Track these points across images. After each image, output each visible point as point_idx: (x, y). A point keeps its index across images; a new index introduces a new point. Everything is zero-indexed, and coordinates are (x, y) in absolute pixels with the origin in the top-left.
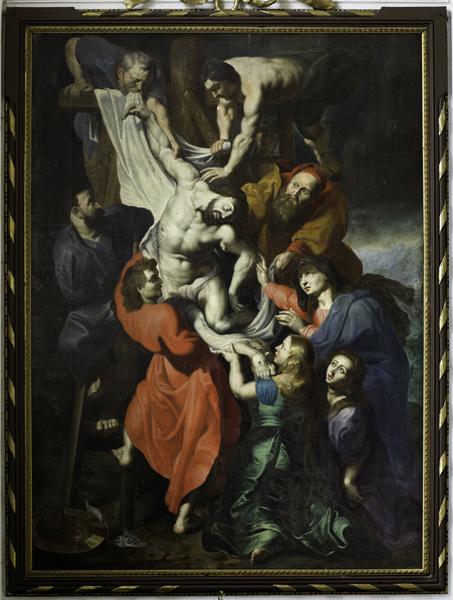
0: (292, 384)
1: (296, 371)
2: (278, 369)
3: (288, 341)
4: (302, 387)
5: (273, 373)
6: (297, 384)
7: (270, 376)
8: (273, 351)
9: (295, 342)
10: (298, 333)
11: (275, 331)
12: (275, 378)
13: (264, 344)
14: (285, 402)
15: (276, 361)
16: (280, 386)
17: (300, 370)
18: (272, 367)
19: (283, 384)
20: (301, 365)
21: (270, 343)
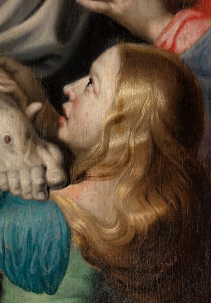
0: (120, 215)
1: (138, 171)
2: (73, 164)
3: (108, 64)
4: (159, 227)
5: (54, 175)
6: (142, 217)
7: (46, 187)
8: (57, 99)
9: (132, 66)
10: (141, 38)
11: (63, 29)
12: (61, 196)
13: (24, 73)
14: (97, 280)
15: (64, 133)
16: (78, 224)
17: (150, 170)
18: (51, 157)
19: (93, 220)
20: (155, 148)
21: (43, 74)
